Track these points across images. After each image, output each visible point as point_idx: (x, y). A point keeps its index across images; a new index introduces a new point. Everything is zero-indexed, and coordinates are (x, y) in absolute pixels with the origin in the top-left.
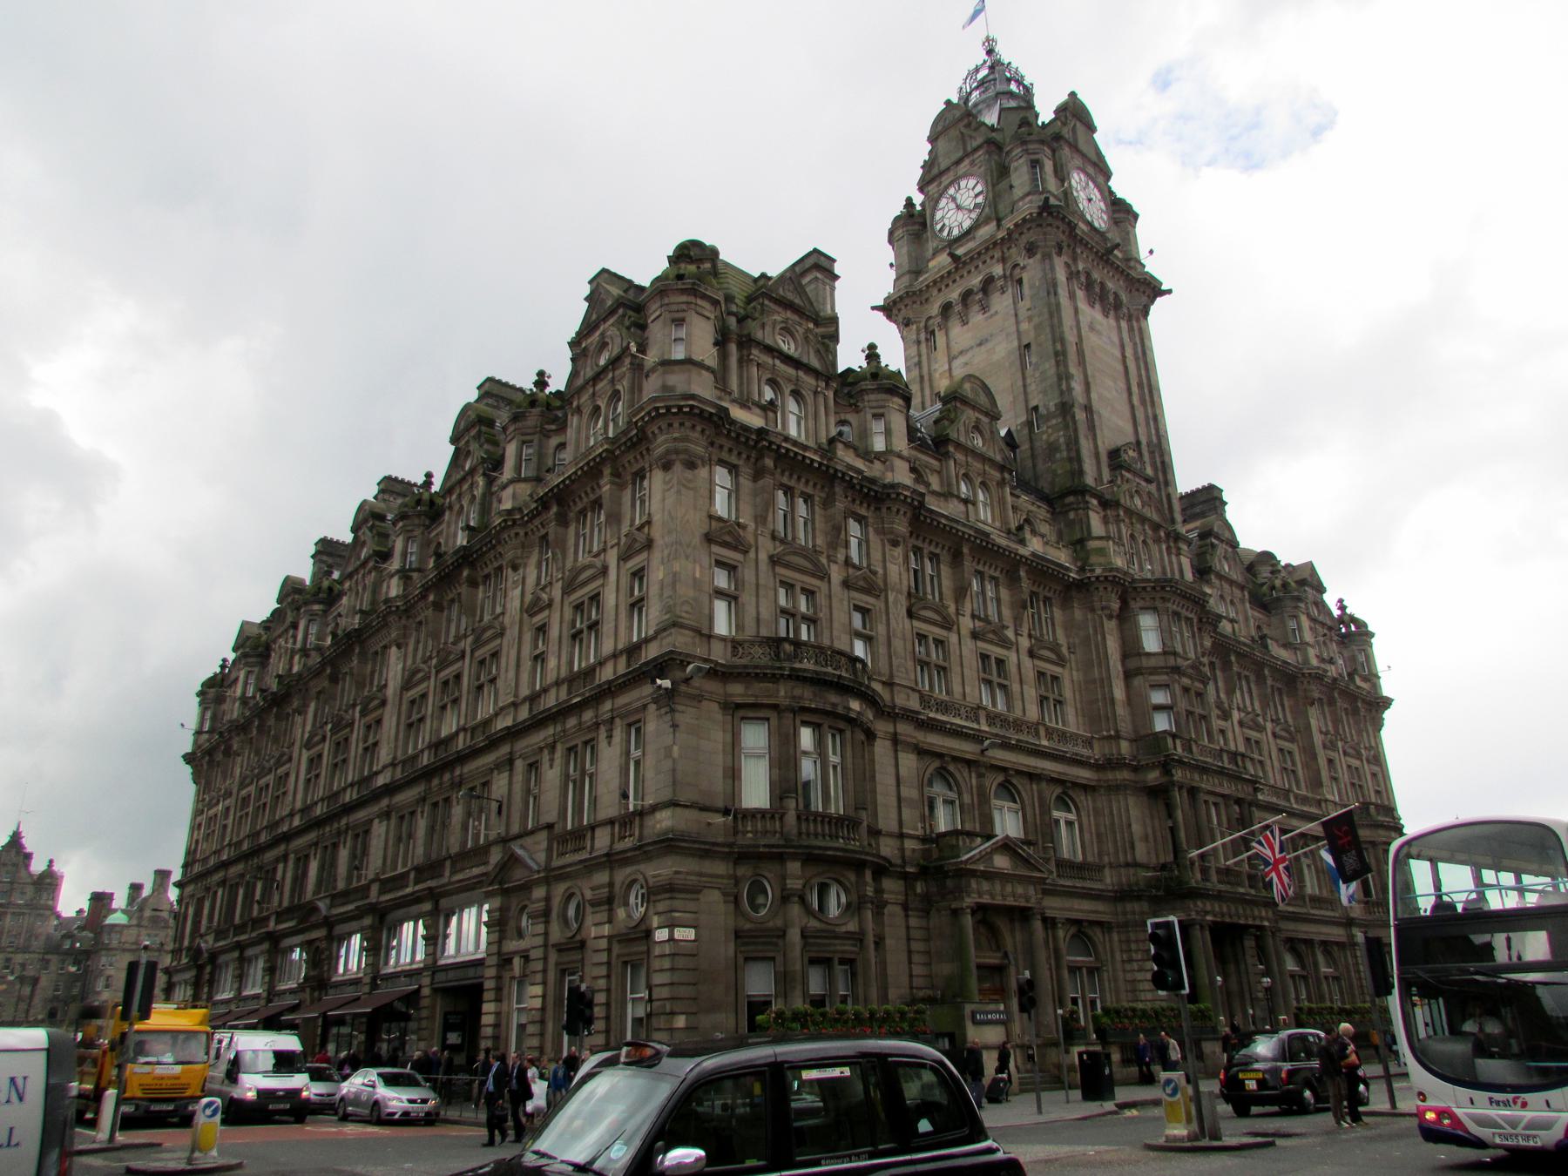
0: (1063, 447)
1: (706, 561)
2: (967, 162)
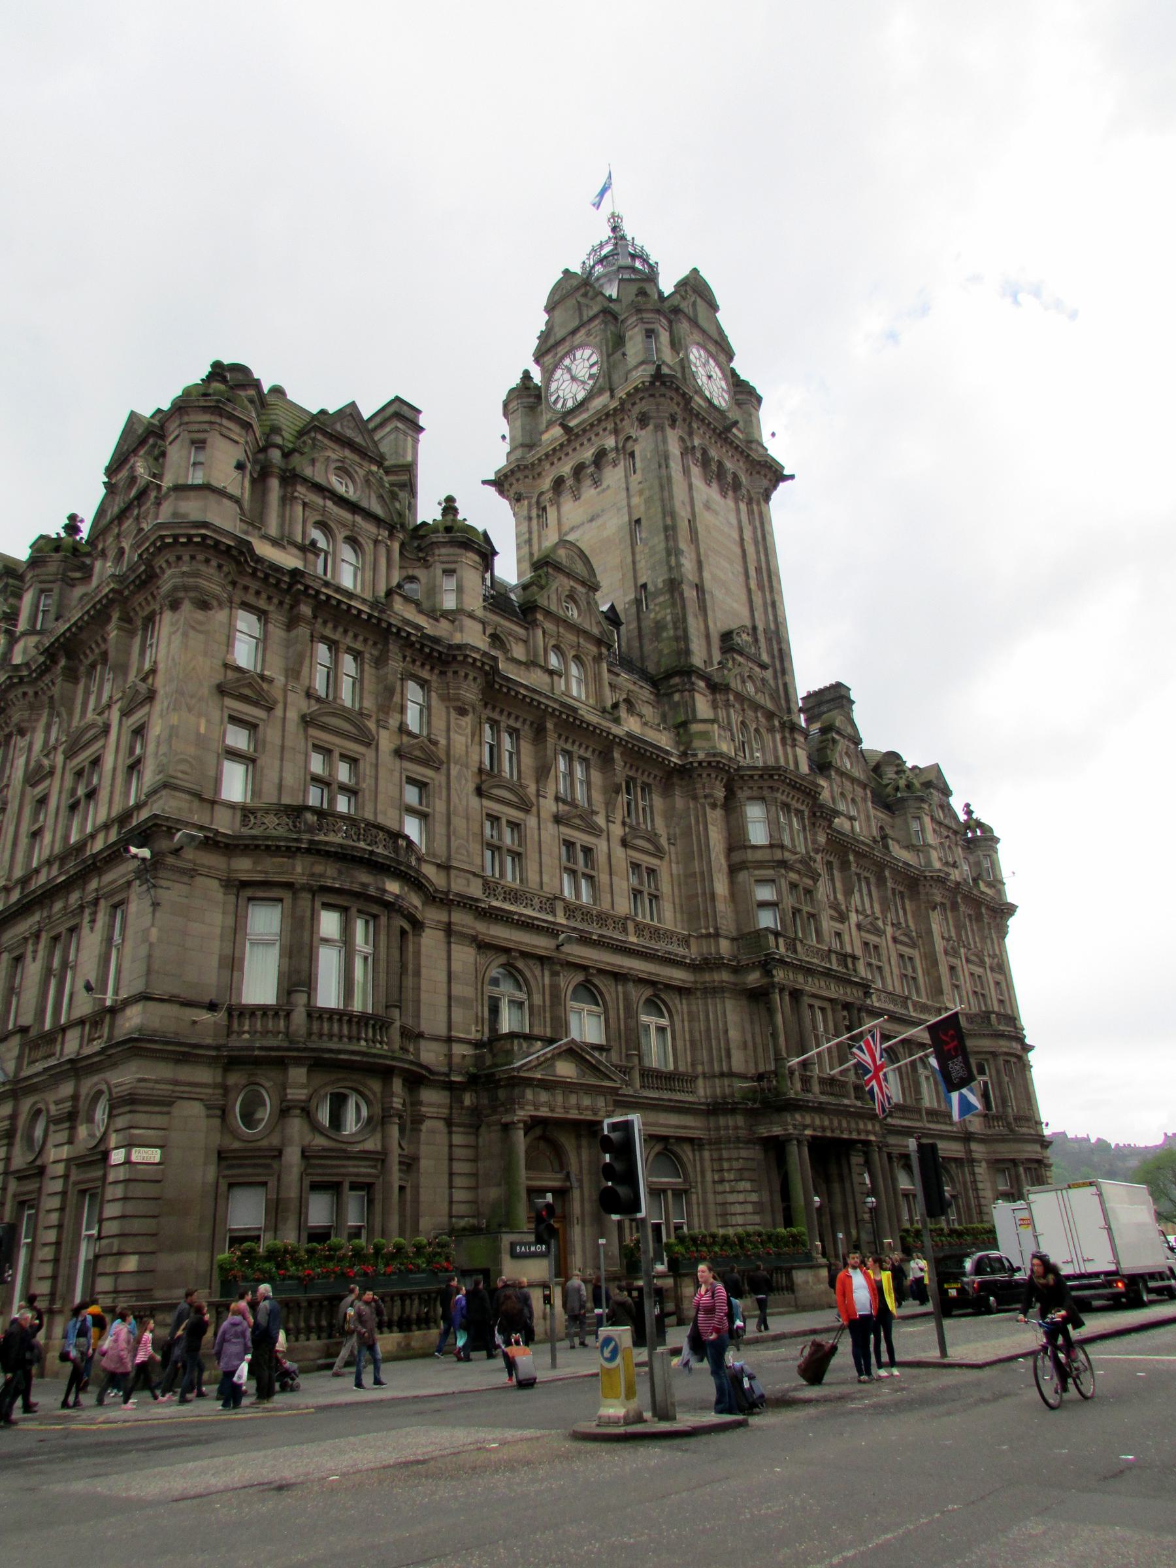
0: (670, 626)
1: (216, 715)
2: (583, 332)
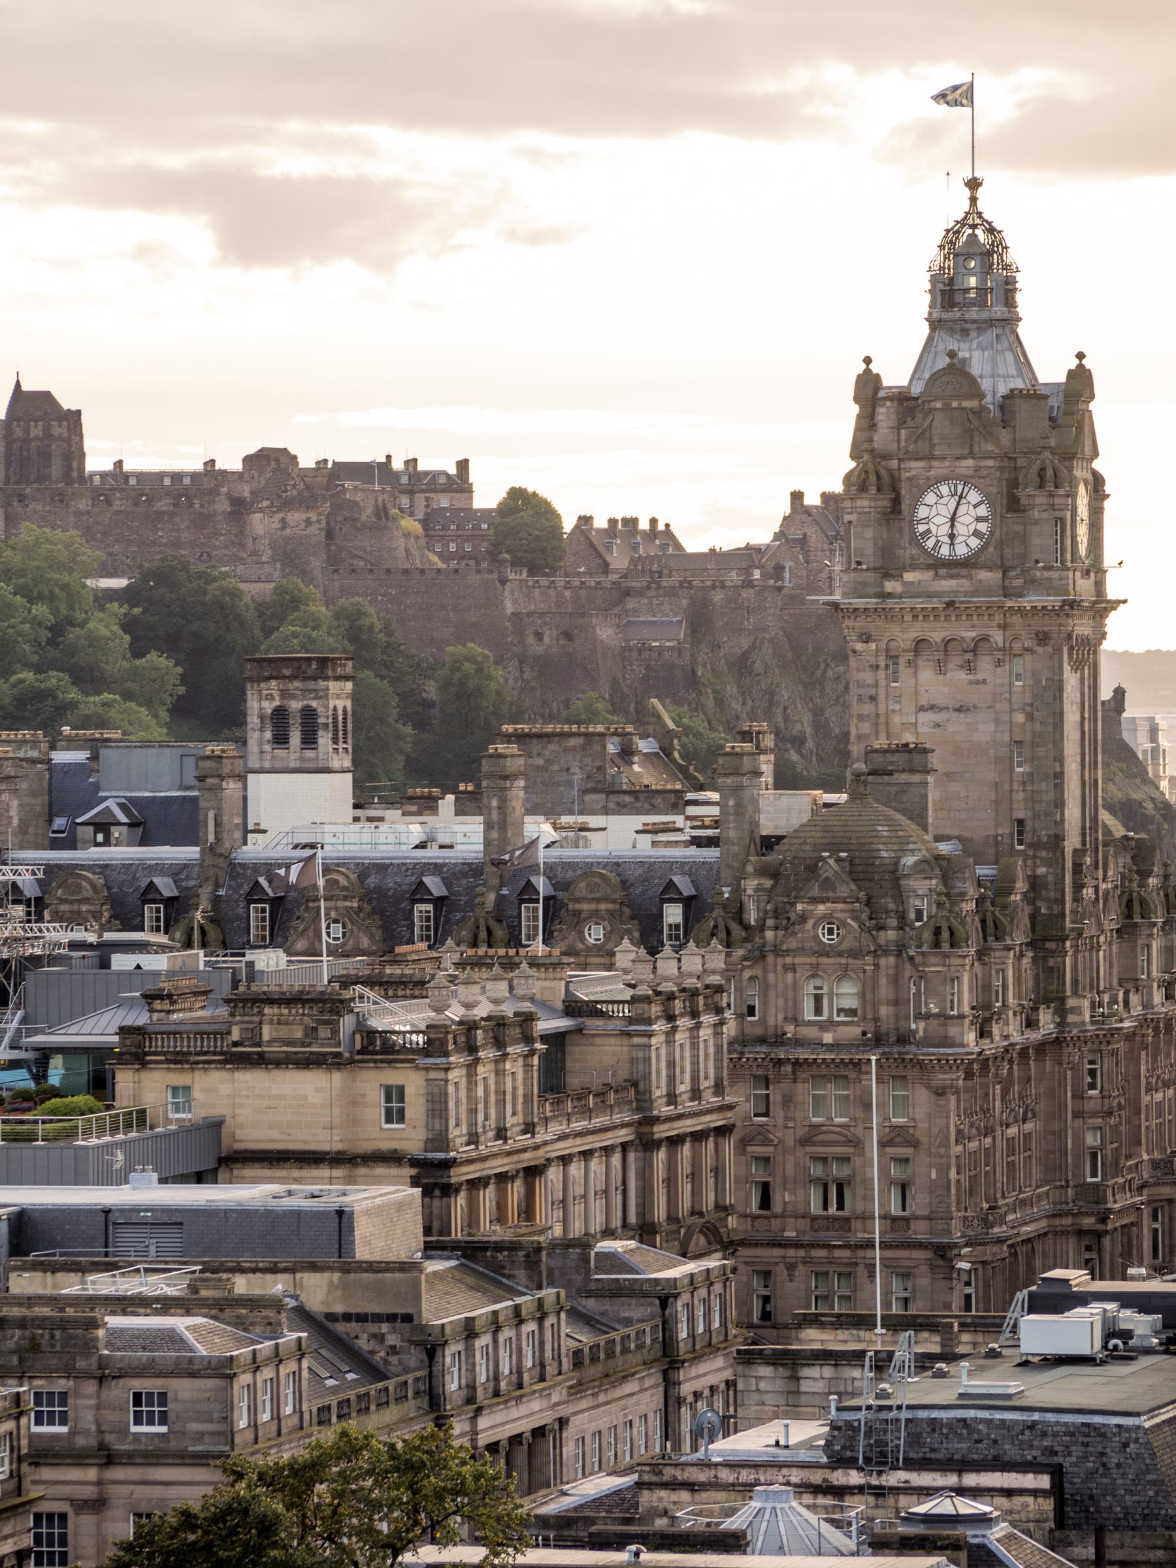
0: (1051, 887)
2: (970, 462)
